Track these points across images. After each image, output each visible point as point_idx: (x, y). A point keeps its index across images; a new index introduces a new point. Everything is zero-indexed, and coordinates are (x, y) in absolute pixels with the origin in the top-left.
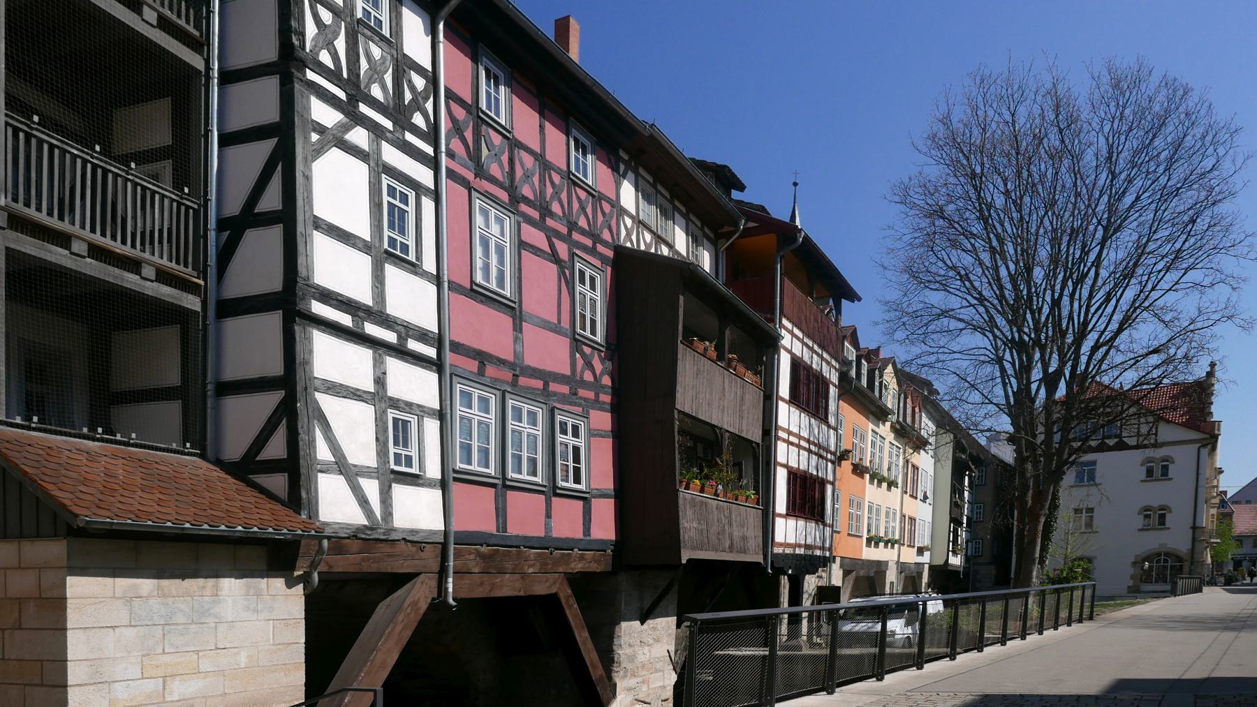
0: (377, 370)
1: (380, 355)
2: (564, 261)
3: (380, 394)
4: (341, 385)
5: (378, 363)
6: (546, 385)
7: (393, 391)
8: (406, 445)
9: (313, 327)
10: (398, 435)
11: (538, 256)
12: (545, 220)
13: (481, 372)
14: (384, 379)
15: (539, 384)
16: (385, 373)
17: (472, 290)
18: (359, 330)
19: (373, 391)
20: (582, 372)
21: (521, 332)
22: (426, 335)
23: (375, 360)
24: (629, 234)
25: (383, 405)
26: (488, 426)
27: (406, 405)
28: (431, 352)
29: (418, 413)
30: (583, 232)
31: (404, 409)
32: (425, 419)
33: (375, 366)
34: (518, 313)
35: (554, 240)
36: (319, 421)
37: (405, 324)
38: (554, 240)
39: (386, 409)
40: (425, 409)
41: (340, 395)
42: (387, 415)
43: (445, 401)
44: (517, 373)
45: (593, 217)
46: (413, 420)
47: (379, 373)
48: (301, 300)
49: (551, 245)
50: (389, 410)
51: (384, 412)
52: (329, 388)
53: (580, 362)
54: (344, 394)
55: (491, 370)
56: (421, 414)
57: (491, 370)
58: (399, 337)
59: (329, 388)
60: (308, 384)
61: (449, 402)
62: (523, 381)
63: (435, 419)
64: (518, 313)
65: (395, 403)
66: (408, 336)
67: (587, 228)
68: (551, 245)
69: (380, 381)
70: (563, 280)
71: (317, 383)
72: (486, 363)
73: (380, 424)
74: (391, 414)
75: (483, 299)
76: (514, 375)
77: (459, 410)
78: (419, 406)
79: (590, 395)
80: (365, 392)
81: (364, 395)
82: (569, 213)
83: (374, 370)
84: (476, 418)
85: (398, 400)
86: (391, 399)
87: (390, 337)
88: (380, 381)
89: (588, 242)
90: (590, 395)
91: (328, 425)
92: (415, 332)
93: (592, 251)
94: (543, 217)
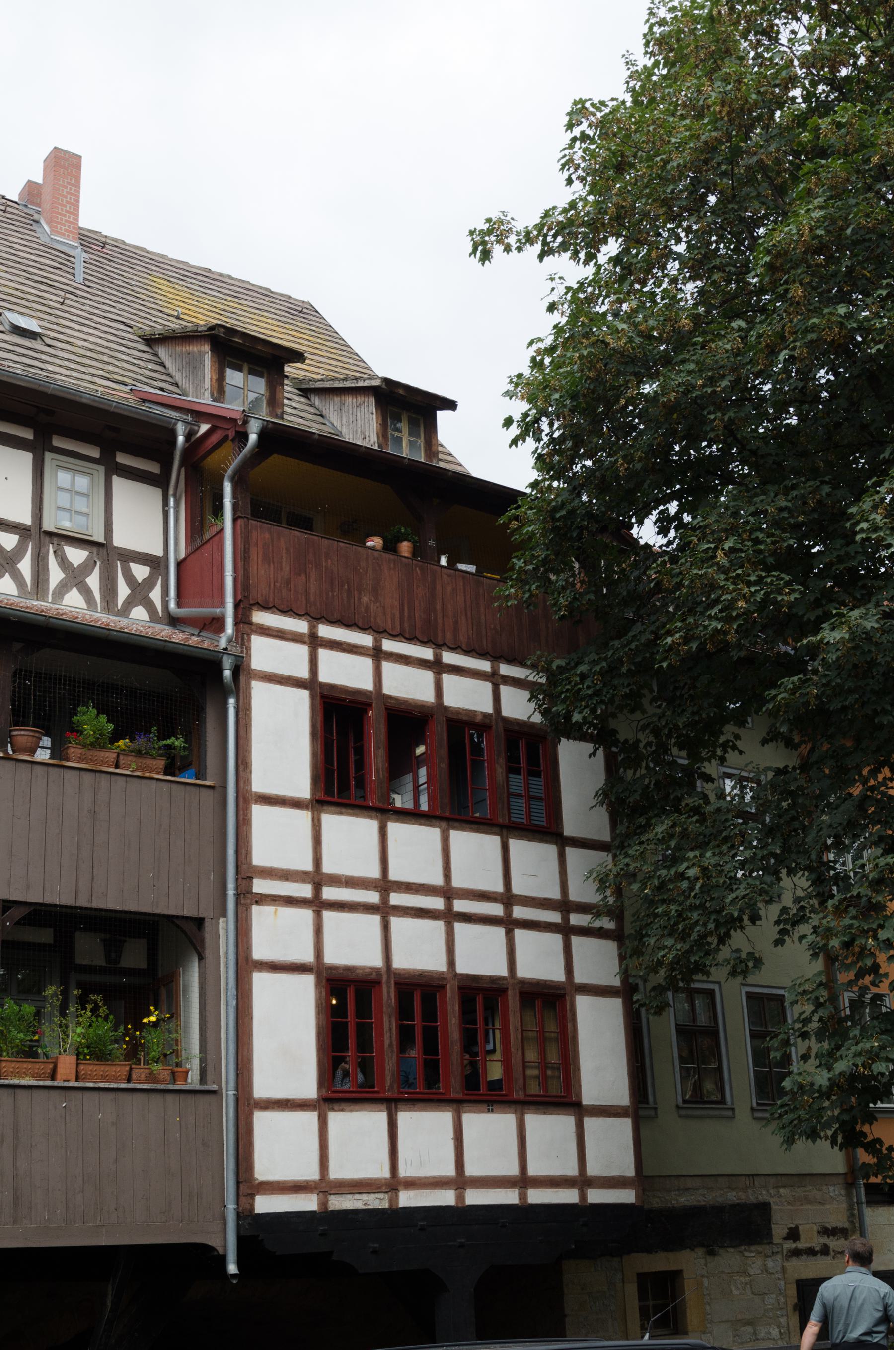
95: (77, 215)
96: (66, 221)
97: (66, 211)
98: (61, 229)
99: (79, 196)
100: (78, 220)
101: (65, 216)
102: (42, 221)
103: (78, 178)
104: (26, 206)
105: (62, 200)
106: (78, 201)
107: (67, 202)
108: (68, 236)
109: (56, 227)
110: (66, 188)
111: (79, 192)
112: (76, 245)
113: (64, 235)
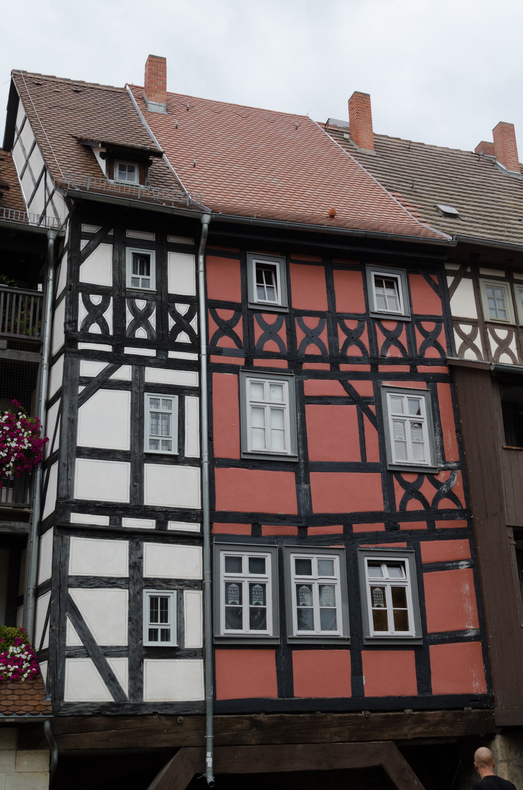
0: (132, 557)
1: (137, 543)
2: (369, 398)
3: (135, 577)
4: (95, 578)
6: (348, 528)
8: (165, 618)
10: (157, 612)
11: (330, 404)
12: (338, 368)
13: (256, 533)
15: (338, 529)
16: (141, 558)
19: (127, 576)
20: (404, 503)
21: (307, 482)
23: (131, 548)
24: (468, 341)
25: (138, 587)
26: (264, 586)
28: (194, 527)
29: (177, 587)
30: (394, 361)
31: (161, 586)
32: (185, 592)
33: (130, 554)
34: (302, 466)
35: (351, 382)
36: (70, 612)
37: (164, 510)
38: (351, 382)
41: (93, 586)
42: (141, 595)
44: (302, 525)
45: (409, 343)
47: (135, 559)
49: (348, 388)
50: (145, 591)
51: (140, 593)
53: (399, 493)
54: (98, 584)
55: (267, 530)
56: (181, 587)
57: (267, 530)
62: (312, 531)
63: (198, 589)
64: (302, 466)
65: (152, 583)
67: (400, 355)
68: (348, 388)
70: (365, 417)
72: (260, 523)
73: (133, 604)
74: (147, 594)
75: (256, 464)
76: (299, 528)
77: (224, 576)
78: (177, 580)
79: (422, 525)
82: (372, 350)
84: (246, 580)
85: (155, 579)
86: (147, 580)
87: (149, 524)
89: (405, 369)
90: (422, 525)
93: (413, 375)
94: (335, 366)
95: (517, 156)
96: (513, 161)
97: (512, 156)
98: (511, 166)
99: (516, 147)
100: (518, 160)
101: (511, 158)
102: (498, 163)
103: (514, 136)
104: (483, 155)
105: (509, 150)
106: (516, 149)
107: (511, 151)
108: (515, 169)
109: (509, 165)
110: (509, 143)
111: (516, 144)
112: (520, 173)
113: (513, 169)
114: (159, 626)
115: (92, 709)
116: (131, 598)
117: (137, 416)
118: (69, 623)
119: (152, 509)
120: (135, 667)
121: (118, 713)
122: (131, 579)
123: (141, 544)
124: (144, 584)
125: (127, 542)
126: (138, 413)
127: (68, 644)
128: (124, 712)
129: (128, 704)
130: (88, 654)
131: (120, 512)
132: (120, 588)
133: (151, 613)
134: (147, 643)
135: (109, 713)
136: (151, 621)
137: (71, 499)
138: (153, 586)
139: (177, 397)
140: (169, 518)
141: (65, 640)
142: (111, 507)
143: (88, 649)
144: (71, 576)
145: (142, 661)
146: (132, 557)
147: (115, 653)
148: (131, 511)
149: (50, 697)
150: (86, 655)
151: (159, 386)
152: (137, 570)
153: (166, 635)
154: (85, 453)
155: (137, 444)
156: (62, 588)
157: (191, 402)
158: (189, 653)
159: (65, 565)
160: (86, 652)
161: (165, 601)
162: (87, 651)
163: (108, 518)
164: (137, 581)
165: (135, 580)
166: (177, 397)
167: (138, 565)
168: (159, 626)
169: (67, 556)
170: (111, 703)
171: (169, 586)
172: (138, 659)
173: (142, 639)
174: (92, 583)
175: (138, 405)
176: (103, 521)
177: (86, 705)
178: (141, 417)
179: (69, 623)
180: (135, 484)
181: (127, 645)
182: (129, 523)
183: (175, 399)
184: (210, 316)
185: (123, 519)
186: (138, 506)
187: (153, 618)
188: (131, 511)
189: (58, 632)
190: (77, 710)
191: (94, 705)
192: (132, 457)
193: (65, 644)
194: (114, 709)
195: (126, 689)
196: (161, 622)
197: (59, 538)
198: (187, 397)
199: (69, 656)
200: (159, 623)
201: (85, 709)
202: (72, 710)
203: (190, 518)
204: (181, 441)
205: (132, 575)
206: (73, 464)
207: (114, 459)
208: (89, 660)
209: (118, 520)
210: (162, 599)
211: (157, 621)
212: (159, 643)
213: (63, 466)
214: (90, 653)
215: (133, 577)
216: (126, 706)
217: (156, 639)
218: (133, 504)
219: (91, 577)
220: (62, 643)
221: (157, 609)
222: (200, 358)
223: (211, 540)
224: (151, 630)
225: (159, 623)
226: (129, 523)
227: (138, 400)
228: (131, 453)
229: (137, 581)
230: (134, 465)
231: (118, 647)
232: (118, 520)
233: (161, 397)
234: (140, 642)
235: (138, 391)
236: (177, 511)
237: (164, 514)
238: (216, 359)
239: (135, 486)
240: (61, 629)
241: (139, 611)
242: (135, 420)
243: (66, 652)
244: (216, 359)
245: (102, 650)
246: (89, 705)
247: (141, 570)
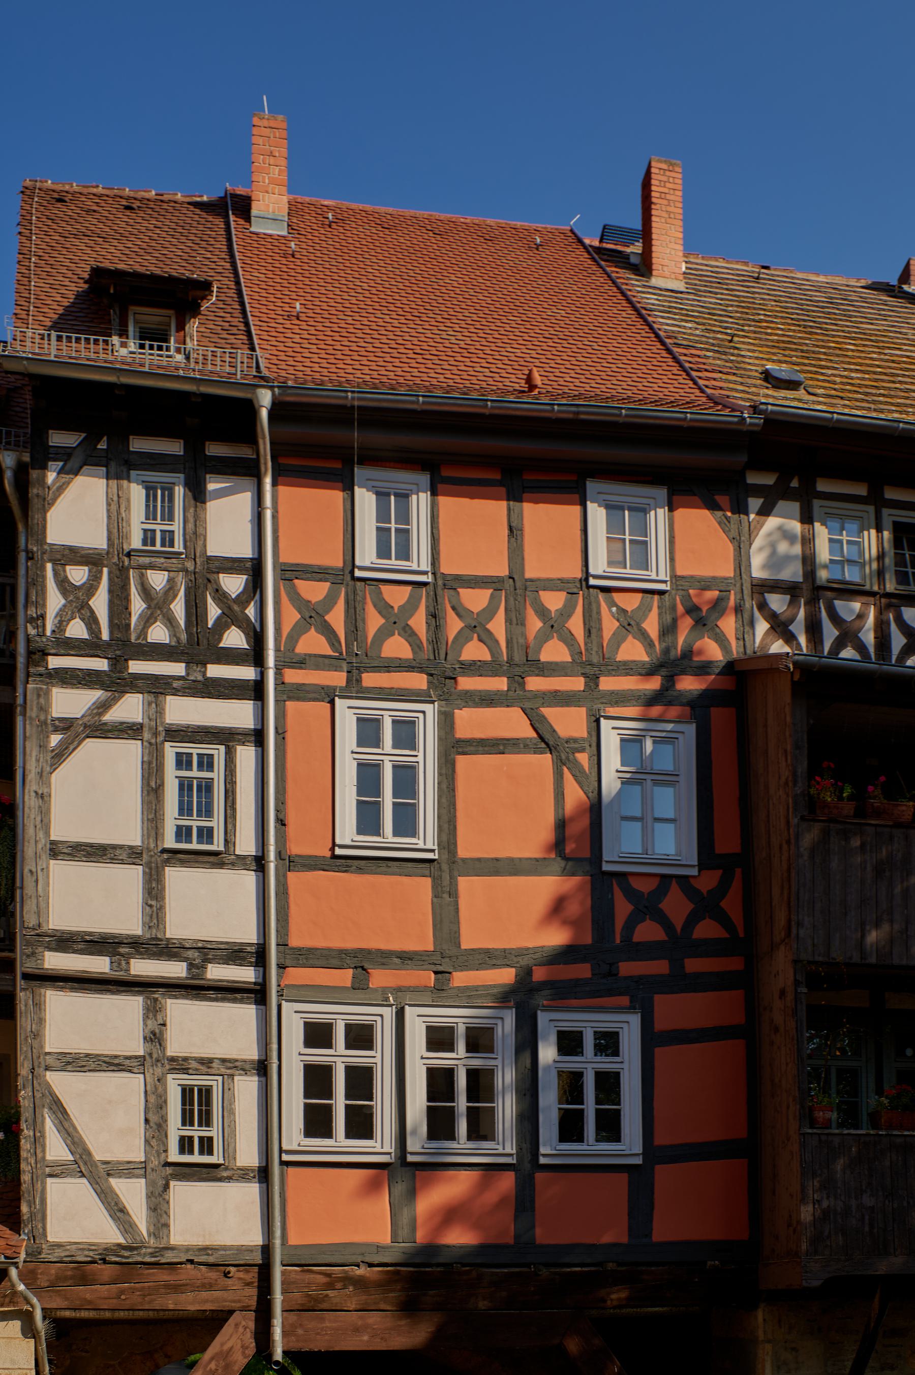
3: (155, 1056)
4: (87, 1055)
5: (153, 1010)
7: (174, 1048)
8: (206, 1120)
9: (46, 987)
14: (161, 1033)
16: (164, 1025)
17: (334, 857)
18: (121, 973)
19: (141, 1053)
22: (241, 951)
25: (159, 1071)
27: (202, 1064)
29: (223, 1071)
31: (197, 1070)
32: (236, 1078)
33: (146, 1017)
37: (200, 945)
39: (164, 1075)
40: (237, 1064)
43: (270, 1043)
46: (216, 1084)
48: (28, 956)
50: (170, 1077)
52: (69, 1063)
54: (93, 1066)
56: (229, 1071)
58: (191, 966)
59: (69, 1063)
60: (36, 1064)
61: (275, 1046)
65: (180, 1065)
66: (207, 960)
69: (155, 1038)
71: (50, 1060)
73: (152, 1099)
78: (224, 1061)
80: (127, 1058)
81: (127, 1062)
83: (145, 1024)
85: (185, 1059)
86: (172, 1059)
87: (176, 970)
88: (155, 1038)
91: (64, 1112)
92: (219, 953)
114: (196, 1132)
115: (91, 1253)
116: (148, 1088)
117: (153, 784)
118: (49, 1125)
119: (180, 943)
120: (157, 1193)
121: (130, 1260)
122: (147, 1057)
123: (163, 1001)
124: (168, 1067)
125: (140, 999)
126: (154, 779)
127: (48, 1157)
128: (140, 1259)
129: (145, 1247)
130: (81, 1172)
131: (127, 950)
132: (130, 1071)
133: (184, 1112)
134: (174, 1156)
135: (117, 1259)
136: (184, 1124)
137: (44, 928)
138: (183, 1069)
139: (222, 748)
140: (209, 959)
141: (44, 1151)
142: (111, 941)
143: (81, 1164)
144: (49, 1053)
145: (166, 1187)
146: (149, 1022)
147: (124, 1171)
148: (143, 948)
149: (25, 1234)
150: (80, 1174)
151: (190, 730)
152: (157, 1044)
153: (207, 1145)
154: (66, 851)
155: (153, 833)
156: (35, 1073)
157: (246, 755)
158: (244, 1174)
159: (38, 1035)
160: (79, 1170)
161: (206, 1094)
162: (79, 1167)
163: (107, 959)
164: (158, 1061)
165: (154, 1059)
166: (222, 748)
167: (158, 1035)
168: (196, 1132)
169: (41, 1021)
170: (119, 1245)
171: (209, 1070)
172: (161, 1182)
173: (166, 1151)
174: (84, 1064)
175: (154, 765)
176: (99, 965)
177: (81, 1246)
178: (160, 786)
179: (49, 1125)
180: (150, 902)
181: (143, 1160)
182: (142, 967)
183: (218, 752)
184: (285, 599)
185: (132, 961)
186: (157, 939)
187: (187, 1120)
188: (143, 948)
189: (33, 1140)
190: (67, 1253)
191: (93, 1248)
192: (145, 856)
193: (44, 1158)
194: (126, 1254)
195: (142, 1227)
196: (198, 1126)
197: (28, 992)
198: (239, 748)
199: (51, 1176)
200: (196, 1127)
201: (80, 1253)
202: (59, 1254)
203: (244, 959)
204: (230, 827)
205: (149, 1052)
206: (44, 870)
207: (114, 860)
208: (84, 1180)
209: (123, 963)
210: (200, 1091)
211: (192, 1124)
212: (196, 1158)
213: (29, 874)
214: (83, 1170)
215: (151, 1055)
216: (144, 1250)
217: (191, 1152)
218: (148, 936)
219: (81, 1055)
220: (40, 1155)
221: (193, 1105)
222: (262, 674)
223: (280, 995)
224: (182, 1139)
225: (196, 1127)
226: (142, 967)
227: (153, 756)
228: (142, 850)
229: (158, 1061)
230: (147, 870)
231: (129, 1162)
232: (123, 963)
233: (195, 750)
234: (163, 1155)
235: (153, 741)
236: (222, 946)
237: (200, 952)
238: (293, 676)
239: (151, 906)
240: (38, 1134)
241: (161, 1108)
242: (148, 792)
243: (48, 1170)
244: (293, 676)
245: (104, 1166)
246: (86, 1247)
247: (163, 1044)
